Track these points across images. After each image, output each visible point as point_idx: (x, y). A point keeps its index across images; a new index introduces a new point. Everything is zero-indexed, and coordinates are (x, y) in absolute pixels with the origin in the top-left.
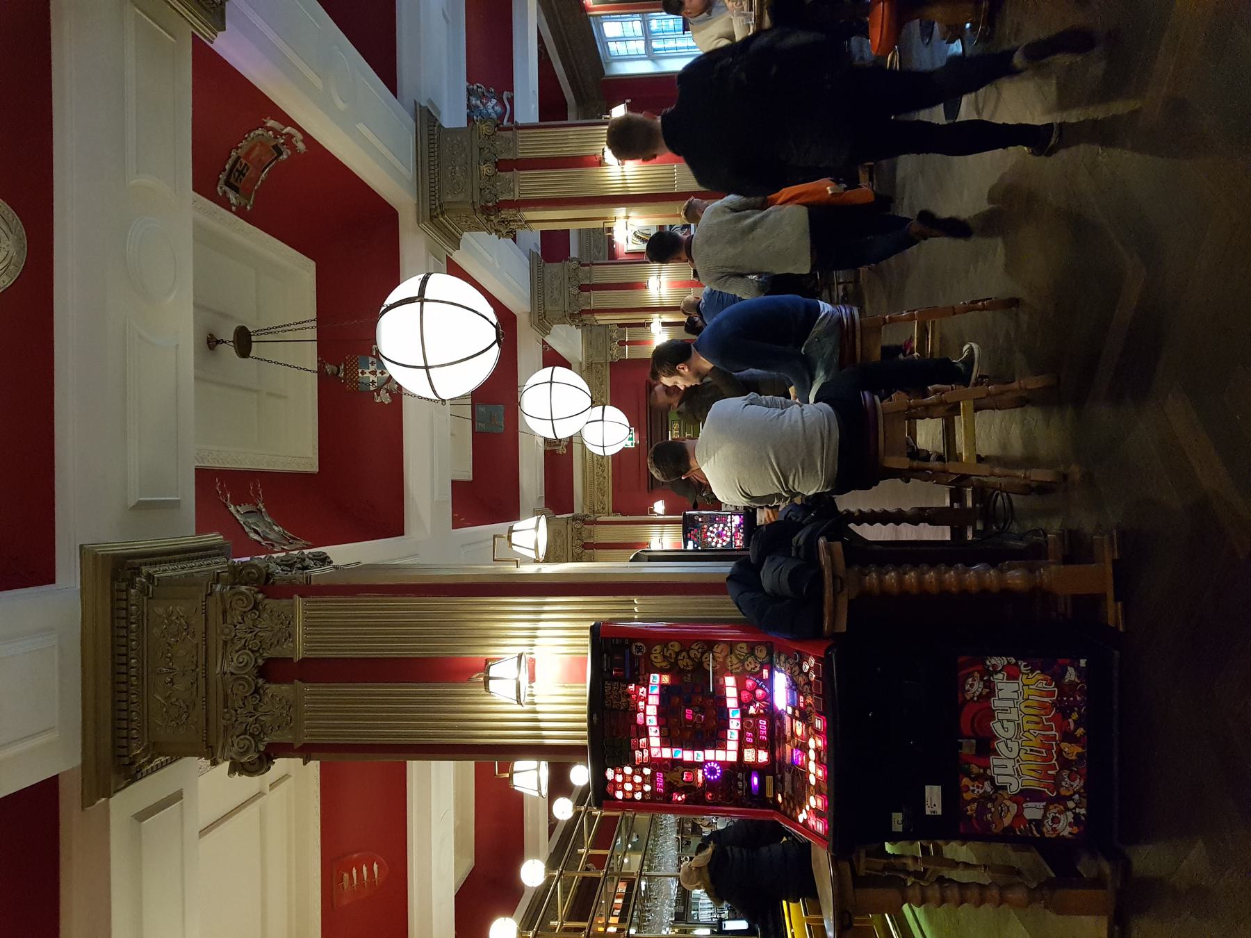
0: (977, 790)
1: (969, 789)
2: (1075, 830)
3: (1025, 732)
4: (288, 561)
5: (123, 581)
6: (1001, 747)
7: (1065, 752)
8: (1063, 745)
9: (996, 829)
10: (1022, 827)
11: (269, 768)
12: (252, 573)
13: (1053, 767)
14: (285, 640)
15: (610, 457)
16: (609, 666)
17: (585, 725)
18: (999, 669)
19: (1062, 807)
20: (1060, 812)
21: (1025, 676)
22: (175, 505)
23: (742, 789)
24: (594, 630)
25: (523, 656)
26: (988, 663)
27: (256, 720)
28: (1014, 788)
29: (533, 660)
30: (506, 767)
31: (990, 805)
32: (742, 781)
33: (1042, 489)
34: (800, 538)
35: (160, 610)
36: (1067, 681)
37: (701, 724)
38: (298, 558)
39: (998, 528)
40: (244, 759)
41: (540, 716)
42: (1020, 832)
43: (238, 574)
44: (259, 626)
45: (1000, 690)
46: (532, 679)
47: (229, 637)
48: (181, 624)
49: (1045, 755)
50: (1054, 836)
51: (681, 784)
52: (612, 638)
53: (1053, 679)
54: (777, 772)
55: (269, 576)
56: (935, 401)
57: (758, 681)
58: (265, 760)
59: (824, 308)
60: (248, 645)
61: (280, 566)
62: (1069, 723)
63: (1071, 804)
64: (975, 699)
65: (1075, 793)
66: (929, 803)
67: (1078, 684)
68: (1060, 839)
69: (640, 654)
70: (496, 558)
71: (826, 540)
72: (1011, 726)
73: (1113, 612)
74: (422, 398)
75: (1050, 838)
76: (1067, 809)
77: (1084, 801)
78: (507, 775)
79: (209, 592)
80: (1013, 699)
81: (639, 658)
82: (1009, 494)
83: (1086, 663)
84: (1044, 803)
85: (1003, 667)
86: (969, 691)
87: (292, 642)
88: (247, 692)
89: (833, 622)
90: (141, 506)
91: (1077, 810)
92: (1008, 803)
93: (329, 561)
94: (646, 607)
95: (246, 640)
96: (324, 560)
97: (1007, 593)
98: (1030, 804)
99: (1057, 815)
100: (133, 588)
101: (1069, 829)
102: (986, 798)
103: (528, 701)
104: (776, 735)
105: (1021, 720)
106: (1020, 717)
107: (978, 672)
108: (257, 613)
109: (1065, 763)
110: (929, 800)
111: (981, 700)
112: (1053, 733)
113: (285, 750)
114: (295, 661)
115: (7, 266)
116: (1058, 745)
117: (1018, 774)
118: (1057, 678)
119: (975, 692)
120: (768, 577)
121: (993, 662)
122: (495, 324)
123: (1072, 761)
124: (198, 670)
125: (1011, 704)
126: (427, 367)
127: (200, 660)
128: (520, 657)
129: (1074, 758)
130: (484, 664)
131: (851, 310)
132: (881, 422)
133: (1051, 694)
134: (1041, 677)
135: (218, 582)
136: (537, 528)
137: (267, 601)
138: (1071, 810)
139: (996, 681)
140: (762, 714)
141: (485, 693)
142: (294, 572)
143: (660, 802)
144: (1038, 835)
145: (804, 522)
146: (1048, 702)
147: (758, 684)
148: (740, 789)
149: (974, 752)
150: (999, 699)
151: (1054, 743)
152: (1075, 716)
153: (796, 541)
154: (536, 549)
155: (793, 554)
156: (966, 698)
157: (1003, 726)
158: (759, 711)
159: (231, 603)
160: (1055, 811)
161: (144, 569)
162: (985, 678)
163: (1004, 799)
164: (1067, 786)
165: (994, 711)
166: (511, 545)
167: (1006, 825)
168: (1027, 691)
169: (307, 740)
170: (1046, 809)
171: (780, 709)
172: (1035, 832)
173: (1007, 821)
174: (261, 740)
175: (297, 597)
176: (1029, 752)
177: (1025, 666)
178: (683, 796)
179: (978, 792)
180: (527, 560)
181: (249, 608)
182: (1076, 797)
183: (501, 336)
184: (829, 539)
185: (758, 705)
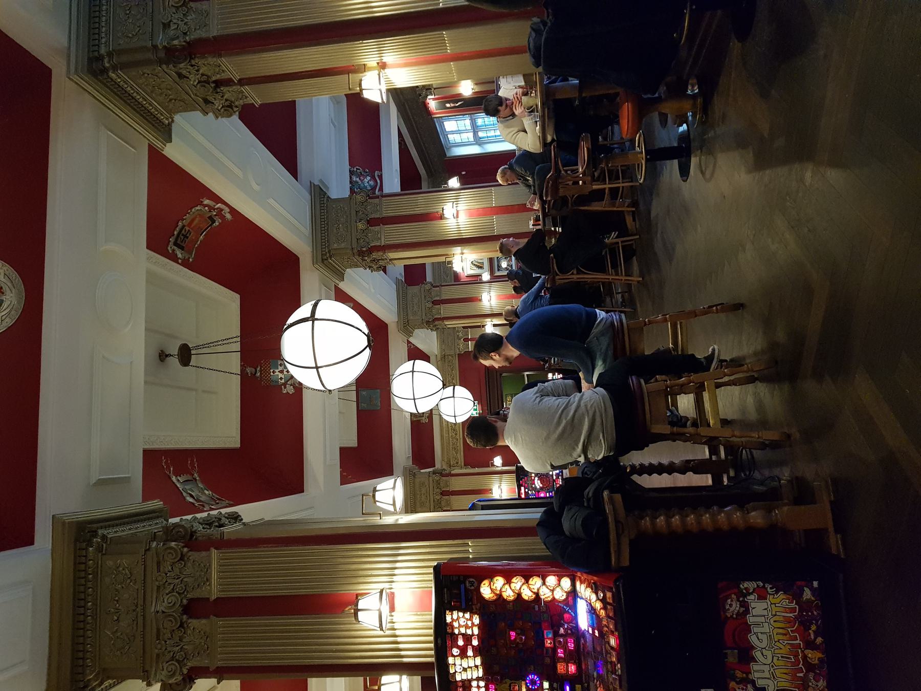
3: (776, 642)
4: (208, 521)
5: (84, 541)
6: (757, 654)
7: (809, 658)
8: (807, 652)
11: (191, 687)
12: (181, 532)
14: (204, 584)
15: (461, 424)
17: (432, 645)
18: (751, 591)
22: (126, 480)
24: (437, 569)
25: (384, 591)
26: (741, 586)
27: (181, 648)
29: (393, 594)
33: (774, 445)
34: (590, 491)
35: (110, 563)
36: (804, 599)
37: (522, 644)
38: (215, 518)
39: (745, 475)
40: (172, 681)
41: (399, 639)
43: (171, 533)
44: (184, 573)
45: (754, 608)
46: (392, 609)
47: (161, 583)
48: (126, 574)
49: (793, 660)
52: (450, 576)
53: (793, 599)
55: (193, 533)
56: (686, 382)
58: (188, 680)
59: (600, 315)
60: (176, 589)
61: (202, 524)
62: (810, 634)
64: (735, 616)
69: (473, 588)
70: (364, 512)
73: (835, 543)
74: (314, 390)
78: (376, 688)
79: (148, 547)
80: (764, 616)
81: (471, 590)
82: (752, 450)
83: (819, 584)
85: (754, 589)
86: (729, 609)
87: (209, 585)
88: (174, 626)
90: (101, 483)
93: (240, 518)
95: (175, 585)
96: (236, 518)
97: (751, 530)
100: (91, 547)
104: (582, 650)
105: (771, 633)
106: (771, 631)
107: (735, 594)
108: (183, 563)
109: (810, 667)
111: (740, 617)
112: (798, 642)
113: (204, 672)
115: (10, 311)
116: (802, 652)
118: (797, 596)
119: (734, 611)
120: (566, 524)
121: (746, 585)
122: (367, 334)
123: (815, 665)
124: (137, 609)
125: (762, 619)
126: (317, 368)
127: (139, 602)
129: (816, 662)
130: (355, 598)
131: (620, 316)
132: (646, 399)
133: (793, 610)
135: (155, 540)
136: (394, 488)
137: (190, 553)
139: (749, 601)
140: (570, 634)
141: (355, 622)
142: (212, 530)
146: (792, 617)
150: (753, 616)
151: (800, 650)
152: (814, 627)
153: (587, 494)
154: (394, 504)
155: (585, 504)
156: (727, 616)
157: (758, 638)
158: (567, 631)
159: (163, 555)
161: (100, 532)
162: (741, 599)
164: (813, 686)
165: (750, 625)
166: (375, 501)
168: (775, 609)
169: (220, 664)
171: (583, 629)
174: (185, 665)
175: (213, 550)
177: (771, 588)
180: (388, 513)
181: (176, 560)
183: (371, 342)
184: (612, 491)
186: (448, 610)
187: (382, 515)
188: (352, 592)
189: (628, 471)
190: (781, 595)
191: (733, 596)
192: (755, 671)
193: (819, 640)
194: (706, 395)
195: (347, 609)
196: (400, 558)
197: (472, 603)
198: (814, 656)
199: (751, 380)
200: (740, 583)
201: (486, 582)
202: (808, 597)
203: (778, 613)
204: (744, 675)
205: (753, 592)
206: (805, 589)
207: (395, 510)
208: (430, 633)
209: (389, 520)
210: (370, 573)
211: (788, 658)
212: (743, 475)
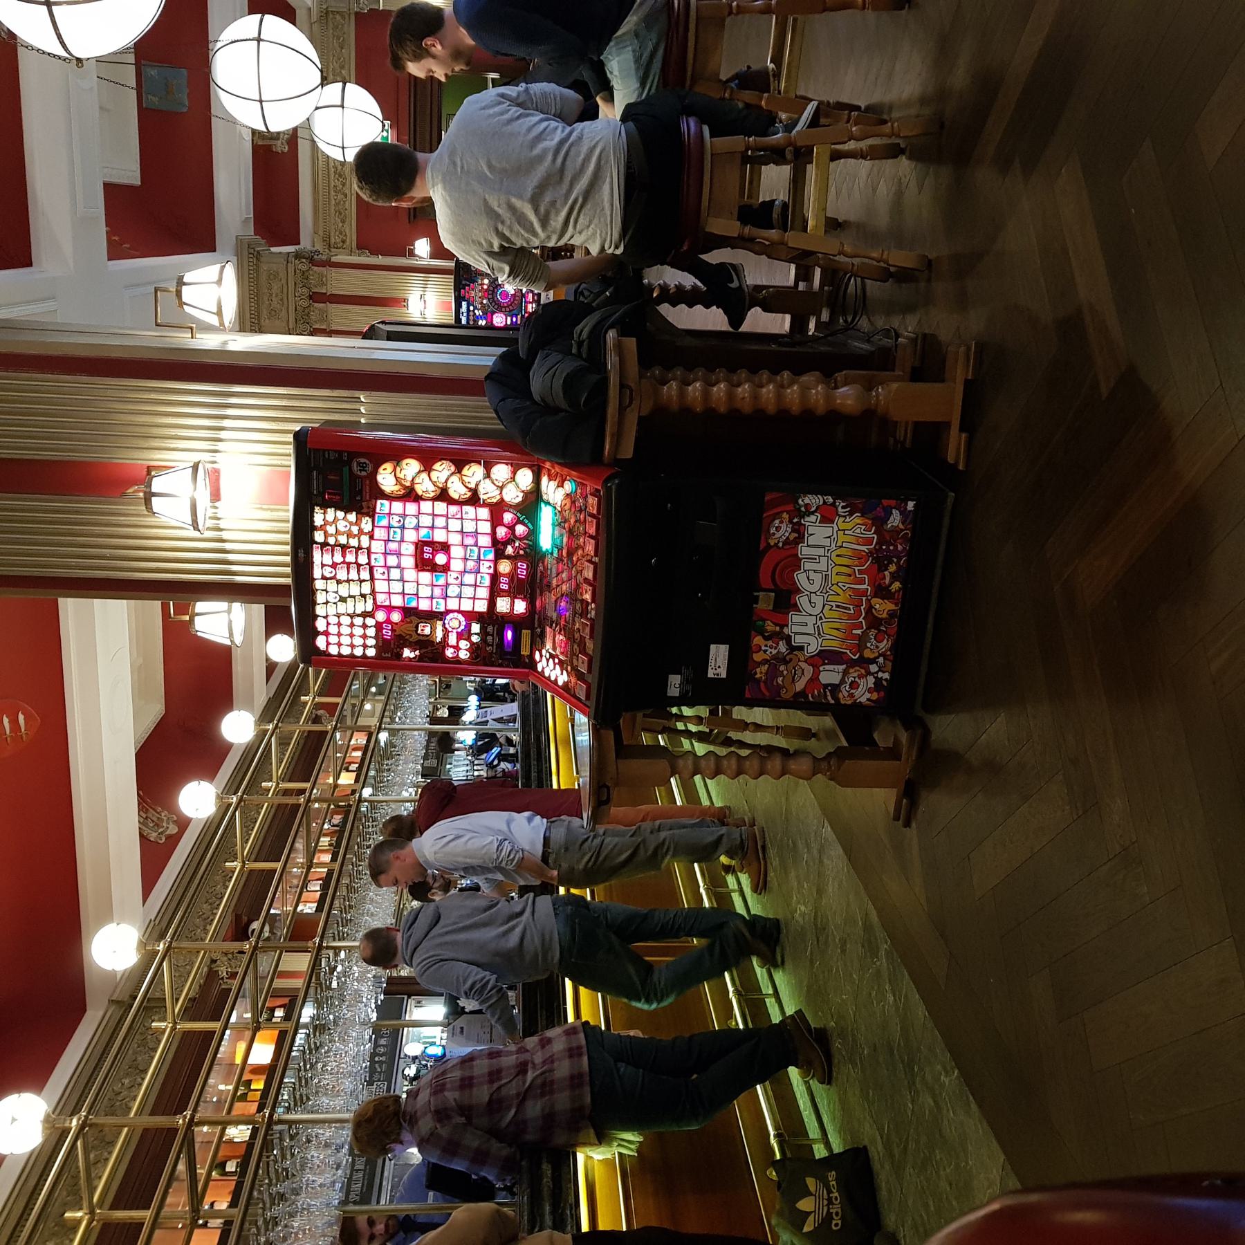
0: (770, 650)
1: (760, 649)
2: (875, 696)
3: (833, 585)
6: (802, 601)
7: (876, 609)
8: (874, 601)
9: (786, 695)
10: (816, 692)
13: (859, 626)
16: (321, 486)
17: (288, 559)
18: (813, 509)
19: (863, 671)
20: (860, 677)
21: (842, 519)
23: (492, 645)
24: (301, 440)
25: (200, 465)
26: (800, 501)
28: (813, 648)
29: (217, 472)
30: (183, 609)
31: (782, 668)
32: (492, 635)
33: (903, 276)
39: (846, 321)
41: (228, 546)
42: (812, 697)
45: (812, 535)
46: (216, 496)
49: (852, 612)
50: (849, 702)
51: (414, 638)
52: (324, 451)
53: (873, 525)
54: (536, 626)
57: (519, 515)
63: (874, 668)
64: (780, 545)
65: (880, 655)
66: (713, 665)
67: (902, 530)
68: (857, 706)
69: (364, 473)
71: (616, 335)
72: (817, 578)
73: (955, 446)
75: (845, 704)
76: (869, 673)
77: (889, 664)
78: (187, 618)
80: (824, 547)
82: (866, 280)
83: (915, 506)
84: (844, 666)
85: (817, 508)
86: (774, 534)
89: (617, 445)
91: (880, 675)
92: (803, 665)
94: (377, 408)
97: (834, 416)
98: (827, 667)
99: (857, 679)
101: (868, 695)
102: (780, 659)
103: (211, 526)
104: (538, 581)
105: (829, 573)
107: (788, 512)
109: (874, 622)
110: (713, 661)
112: (865, 586)
116: (868, 601)
117: (819, 633)
118: (879, 522)
120: (538, 381)
121: (807, 501)
125: (821, 551)
128: (195, 467)
129: (885, 615)
130: (145, 473)
133: (868, 541)
134: (859, 521)
138: (873, 674)
139: (807, 524)
141: (146, 513)
143: (387, 658)
144: (833, 702)
145: (594, 304)
146: (864, 551)
147: (519, 518)
148: (489, 645)
149: (771, 608)
150: (808, 546)
151: (864, 598)
152: (893, 568)
154: (219, 313)
155: (574, 351)
158: (518, 552)
160: (856, 674)
162: (795, 520)
163: (799, 661)
164: (872, 647)
165: (801, 559)
166: (182, 304)
167: (798, 690)
170: (845, 673)
171: (544, 550)
172: (829, 698)
173: (800, 685)
176: (834, 608)
177: (843, 507)
178: (417, 653)
179: (771, 653)
180: (208, 328)
182: (881, 660)
184: (623, 333)
185: (517, 544)
186: (317, 506)
187: (194, 330)
188: (139, 462)
189: (655, 295)
190: (857, 519)
191: (785, 515)
192: (793, 624)
193: (896, 585)
194: (812, 171)
195: (130, 490)
196: (230, 412)
197: (362, 498)
198: (883, 607)
199: (893, 152)
200: (800, 497)
201: (388, 466)
202: (895, 524)
203: (844, 545)
204: (778, 628)
205: (815, 511)
206: (894, 511)
207: (222, 324)
208: (283, 540)
209: (209, 342)
210: (174, 432)
211: (845, 608)
212: (841, 321)
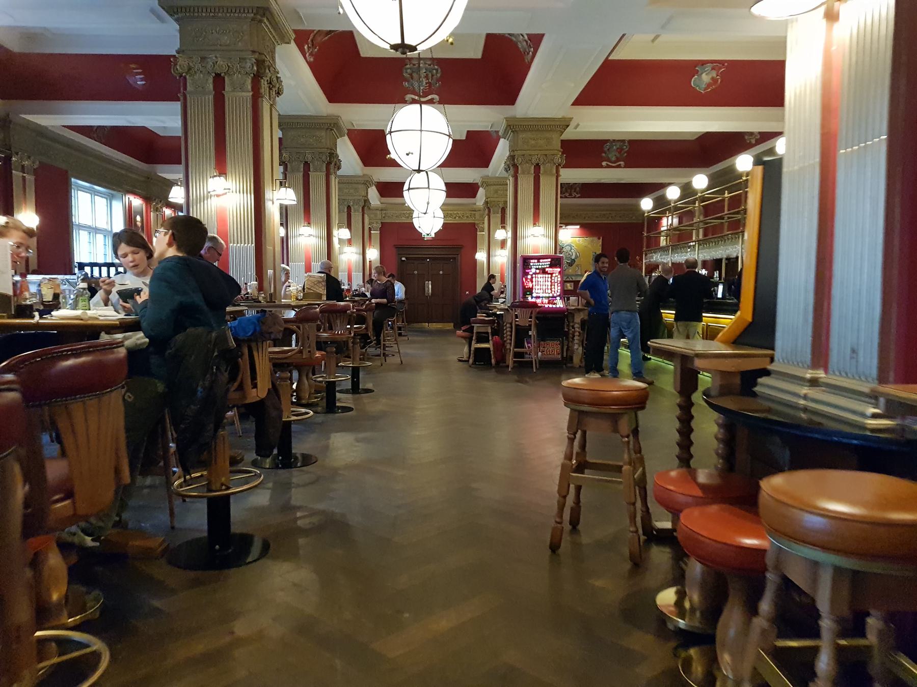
114: (223, 92)
